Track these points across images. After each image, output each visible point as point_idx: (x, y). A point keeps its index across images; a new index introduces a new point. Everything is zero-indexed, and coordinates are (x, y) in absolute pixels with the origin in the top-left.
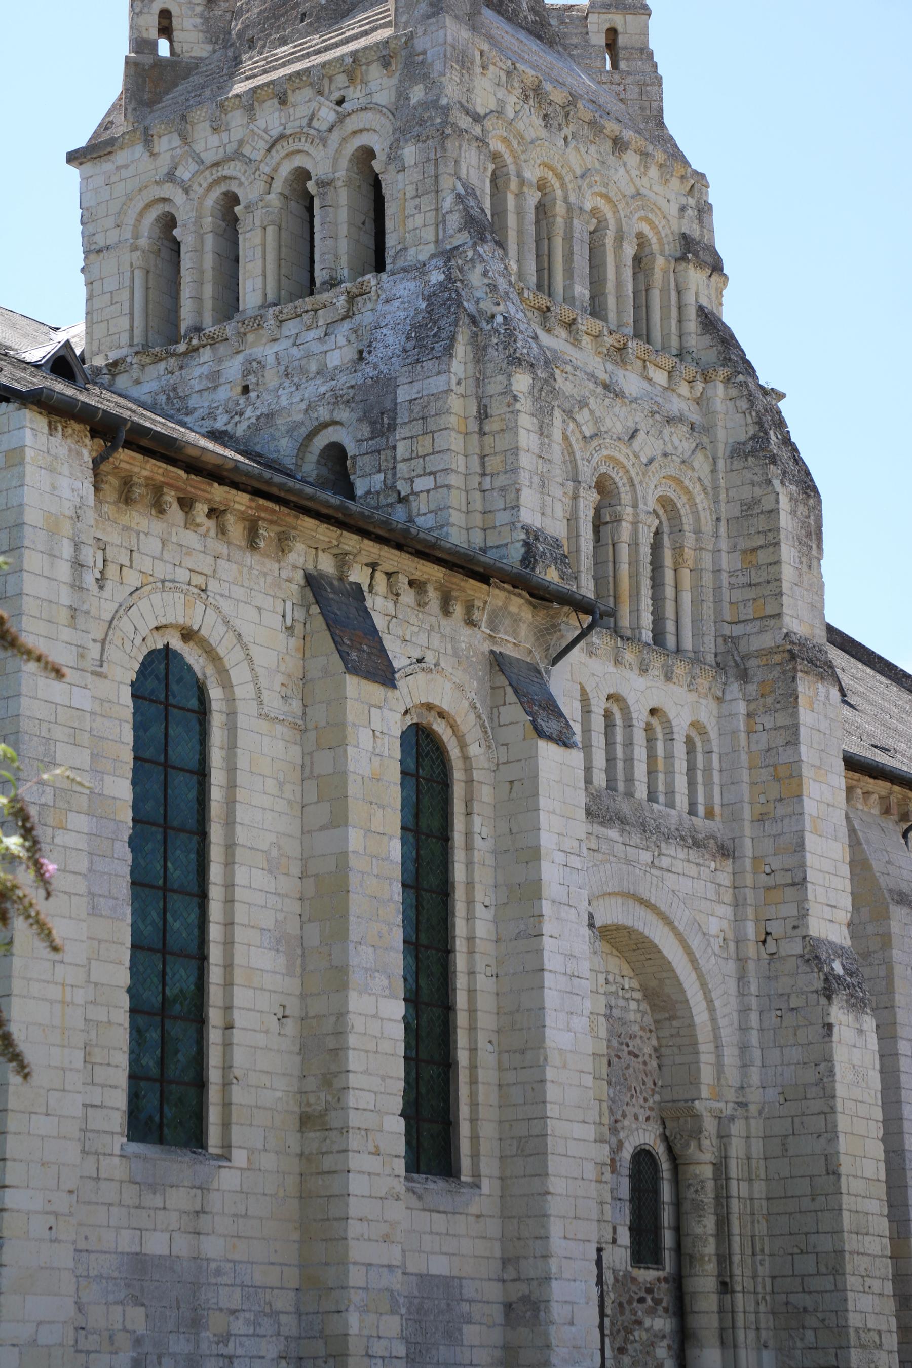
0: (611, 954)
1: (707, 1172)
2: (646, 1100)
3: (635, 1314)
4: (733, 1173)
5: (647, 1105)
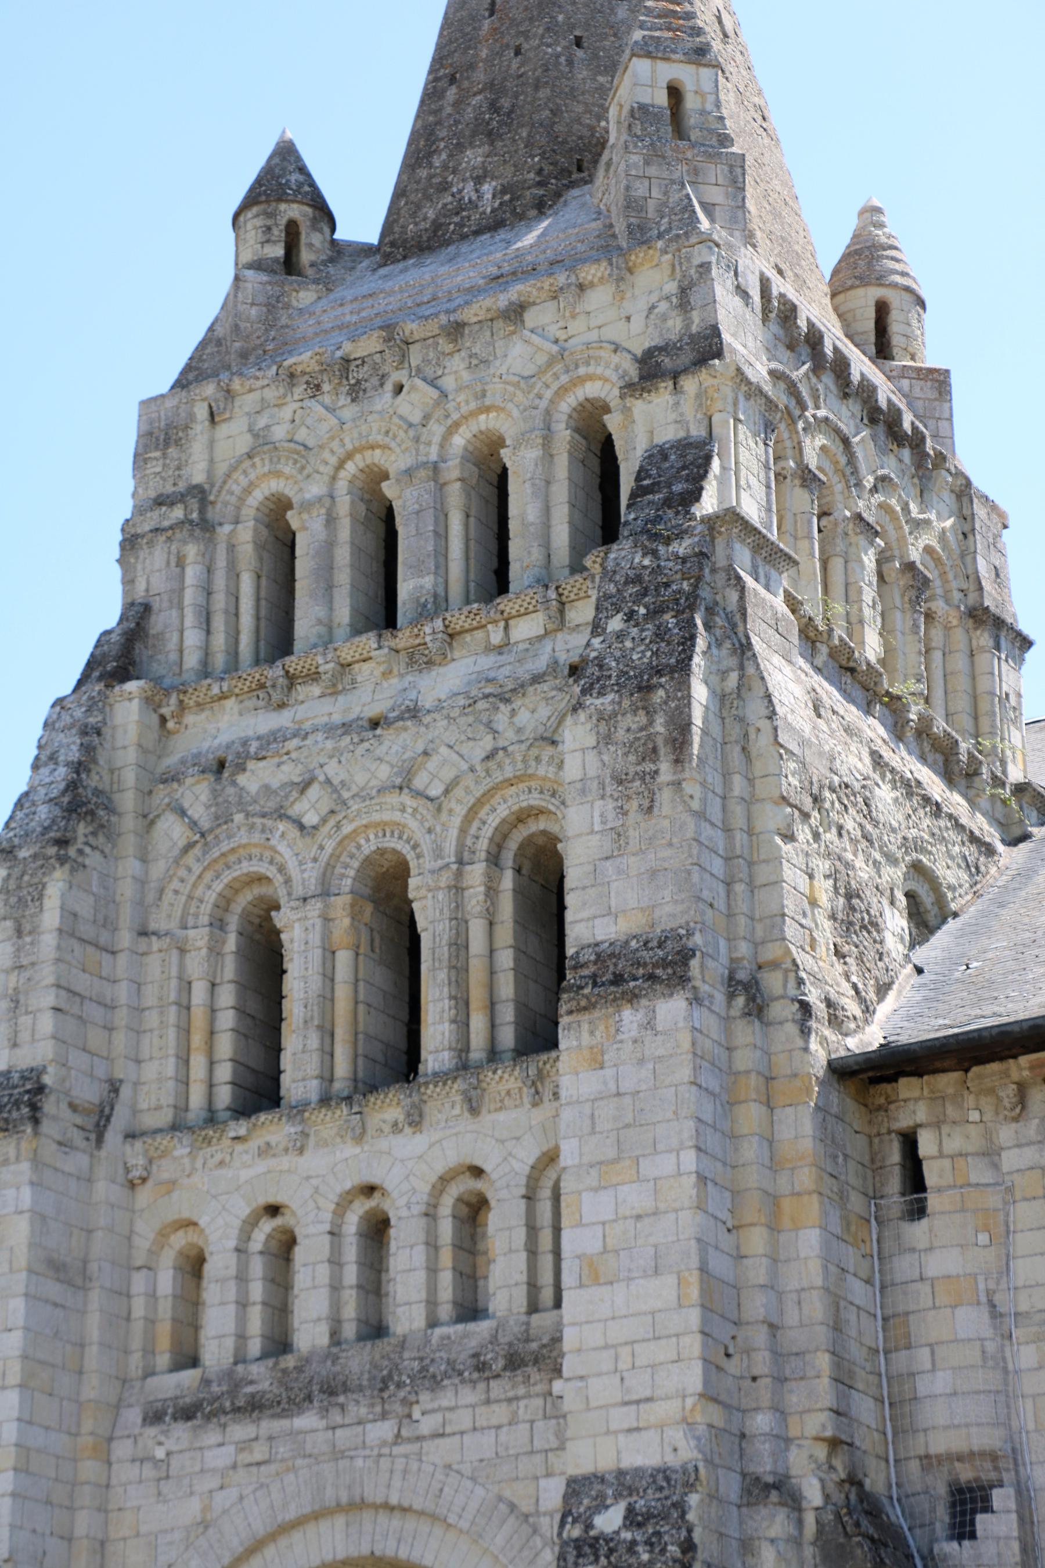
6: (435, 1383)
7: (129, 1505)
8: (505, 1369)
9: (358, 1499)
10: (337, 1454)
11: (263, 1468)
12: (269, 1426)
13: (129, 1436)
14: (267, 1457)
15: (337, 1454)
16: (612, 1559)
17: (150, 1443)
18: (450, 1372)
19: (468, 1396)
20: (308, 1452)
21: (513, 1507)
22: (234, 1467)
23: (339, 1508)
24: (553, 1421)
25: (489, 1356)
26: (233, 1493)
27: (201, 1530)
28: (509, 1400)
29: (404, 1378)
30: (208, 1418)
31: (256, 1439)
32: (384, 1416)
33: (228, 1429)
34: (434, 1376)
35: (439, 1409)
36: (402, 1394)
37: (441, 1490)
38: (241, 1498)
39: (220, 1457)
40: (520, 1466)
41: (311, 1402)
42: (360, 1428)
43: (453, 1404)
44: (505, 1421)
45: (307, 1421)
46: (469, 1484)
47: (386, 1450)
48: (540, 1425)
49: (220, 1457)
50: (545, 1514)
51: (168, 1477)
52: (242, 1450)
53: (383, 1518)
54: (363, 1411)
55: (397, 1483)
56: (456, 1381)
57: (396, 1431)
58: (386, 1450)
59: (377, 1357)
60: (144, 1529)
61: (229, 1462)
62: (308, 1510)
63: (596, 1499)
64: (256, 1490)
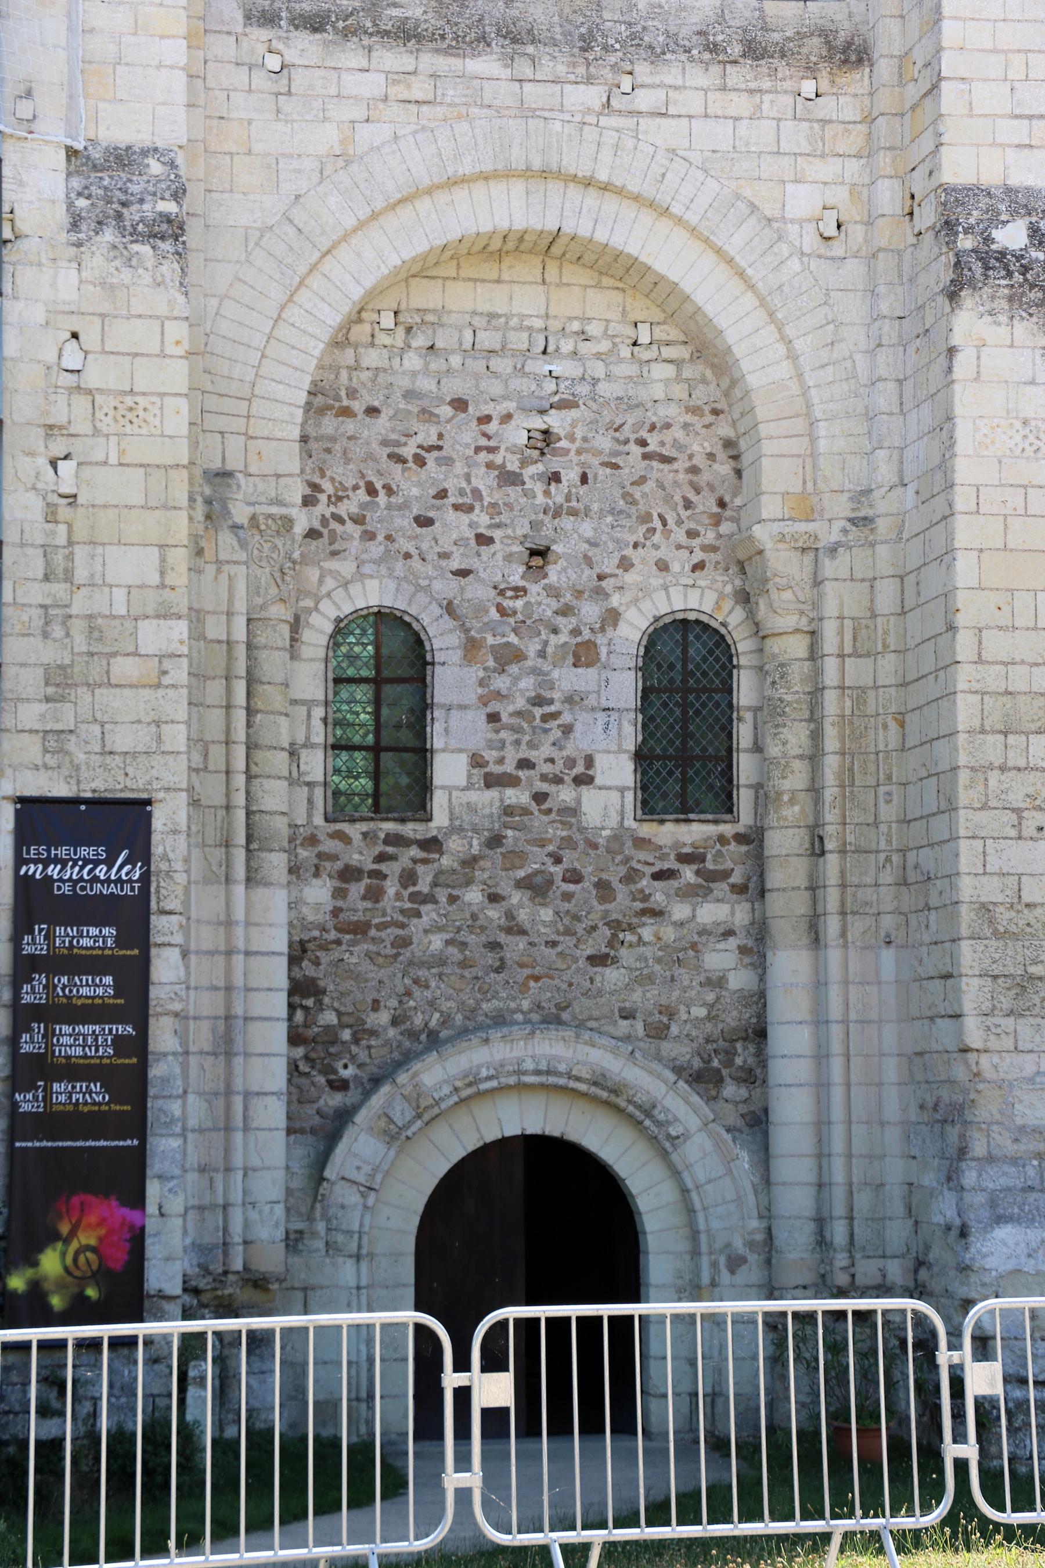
0: (598, 286)
1: (796, 647)
2: (691, 534)
3: (646, 898)
4: (830, 643)
5: (696, 542)
6: (656, 55)
7: (234, 115)
8: (744, 56)
9: (555, 169)
10: (526, 112)
11: (424, 108)
12: (429, 61)
13: (229, 33)
14: (430, 97)
15: (526, 112)
16: (1029, 276)
17: (261, 49)
18: (672, 46)
19: (698, 77)
20: (486, 102)
21: (753, 208)
22: (386, 99)
23: (527, 173)
24: (806, 124)
25: (720, 38)
26: (386, 131)
27: (341, 163)
28: (751, 92)
29: (611, 41)
30: (347, 33)
31: (415, 73)
32: (589, 80)
33: (374, 54)
34: (650, 47)
35: (660, 85)
36: (612, 59)
37: (664, 175)
38: (396, 137)
39: (372, 85)
40: (763, 166)
41: (489, 45)
42: (557, 88)
43: (680, 83)
44: (746, 114)
45: (485, 65)
46: (700, 175)
47: (591, 119)
48: (788, 126)
49: (372, 85)
50: (792, 221)
51: (289, 93)
52: (396, 82)
53: (574, 192)
54: (561, 69)
55: (606, 156)
56: (683, 57)
57: (605, 99)
58: (591, 119)
59: (567, 10)
60: (257, 148)
61: (379, 92)
62: (488, 167)
63: (988, 211)
64: (416, 132)
